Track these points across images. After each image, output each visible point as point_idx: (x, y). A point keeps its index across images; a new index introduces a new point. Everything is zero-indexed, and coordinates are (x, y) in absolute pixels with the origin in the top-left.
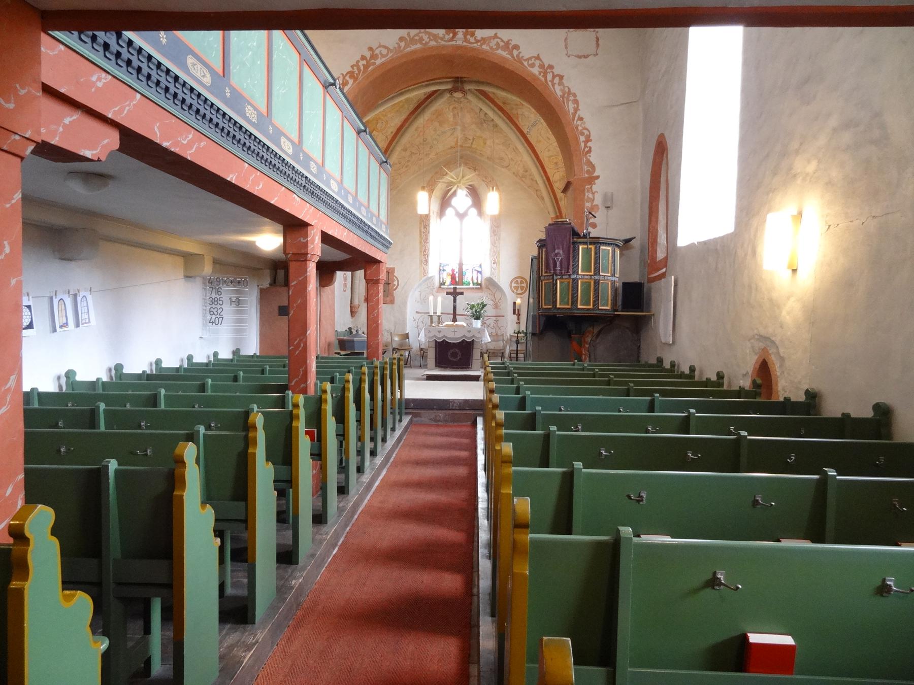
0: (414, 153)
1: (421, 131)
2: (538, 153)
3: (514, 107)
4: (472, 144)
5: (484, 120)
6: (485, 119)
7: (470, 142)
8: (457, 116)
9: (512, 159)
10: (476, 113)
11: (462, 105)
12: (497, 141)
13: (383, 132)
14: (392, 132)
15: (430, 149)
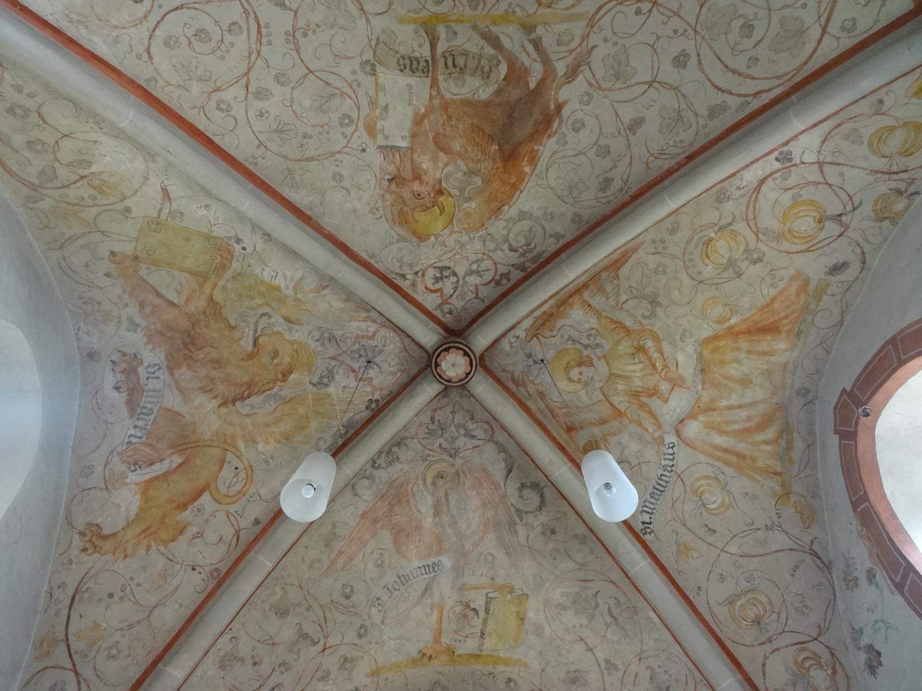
0: (306, 636)
1: (340, 553)
2: (691, 597)
3: (597, 431)
4: (482, 634)
5: (517, 511)
6: (520, 507)
7: (477, 623)
8: (445, 508)
9: (608, 662)
10: (496, 486)
11: (458, 462)
12: (557, 594)
13: (232, 509)
14: (257, 522)
15: (360, 636)
